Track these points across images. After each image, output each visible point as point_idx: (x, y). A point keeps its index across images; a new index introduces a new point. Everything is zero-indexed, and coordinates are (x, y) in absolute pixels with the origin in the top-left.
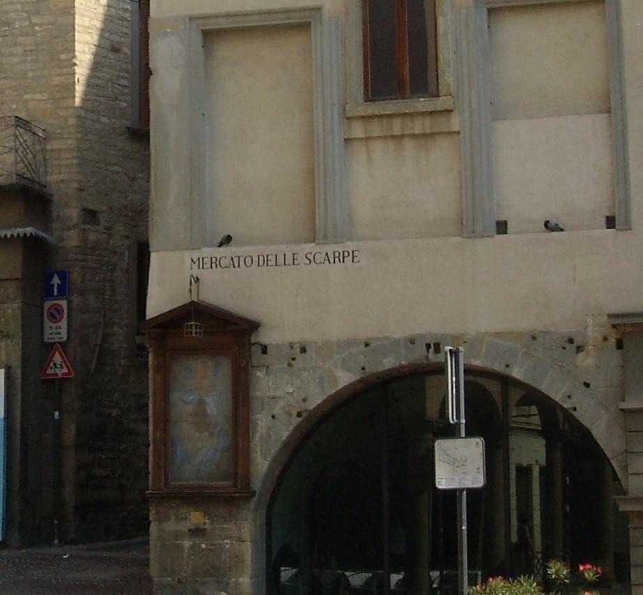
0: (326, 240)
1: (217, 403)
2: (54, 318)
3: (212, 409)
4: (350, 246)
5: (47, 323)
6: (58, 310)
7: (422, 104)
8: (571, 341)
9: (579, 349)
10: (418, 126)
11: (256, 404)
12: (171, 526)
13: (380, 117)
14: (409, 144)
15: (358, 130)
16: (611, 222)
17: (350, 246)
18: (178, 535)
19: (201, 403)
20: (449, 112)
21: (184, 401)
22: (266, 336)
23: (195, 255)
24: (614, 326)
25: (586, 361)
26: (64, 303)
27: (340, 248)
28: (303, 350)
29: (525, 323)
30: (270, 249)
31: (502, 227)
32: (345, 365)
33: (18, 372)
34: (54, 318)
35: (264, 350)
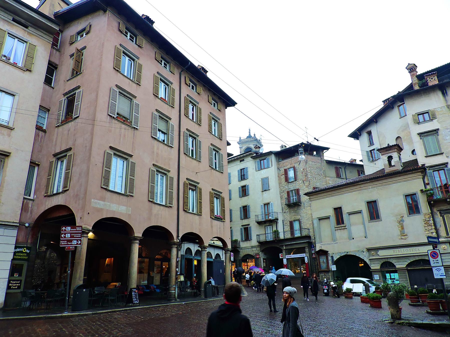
0: (334, 241)
1: (325, 261)
2: (313, 250)
3: (325, 261)
4: (337, 242)
5: (312, 251)
6: (313, 249)
7: (343, 225)
8: (362, 251)
9: (364, 252)
10: (343, 228)
11: (329, 260)
12: (322, 275)
13: (338, 227)
14: (342, 230)
15: (336, 229)
16: (365, 237)
17: (337, 242)
18: (323, 275)
19: (323, 260)
20: (346, 226)
21: (321, 260)
22: (329, 253)
23: (321, 244)
24: (367, 249)
25: (365, 253)
26: (314, 248)
27: (336, 242)
28: (333, 254)
29: (357, 249)
30: (328, 243)
31: (353, 239)
32: (338, 255)
33: (309, 257)
34: (313, 250)
35: (329, 254)
